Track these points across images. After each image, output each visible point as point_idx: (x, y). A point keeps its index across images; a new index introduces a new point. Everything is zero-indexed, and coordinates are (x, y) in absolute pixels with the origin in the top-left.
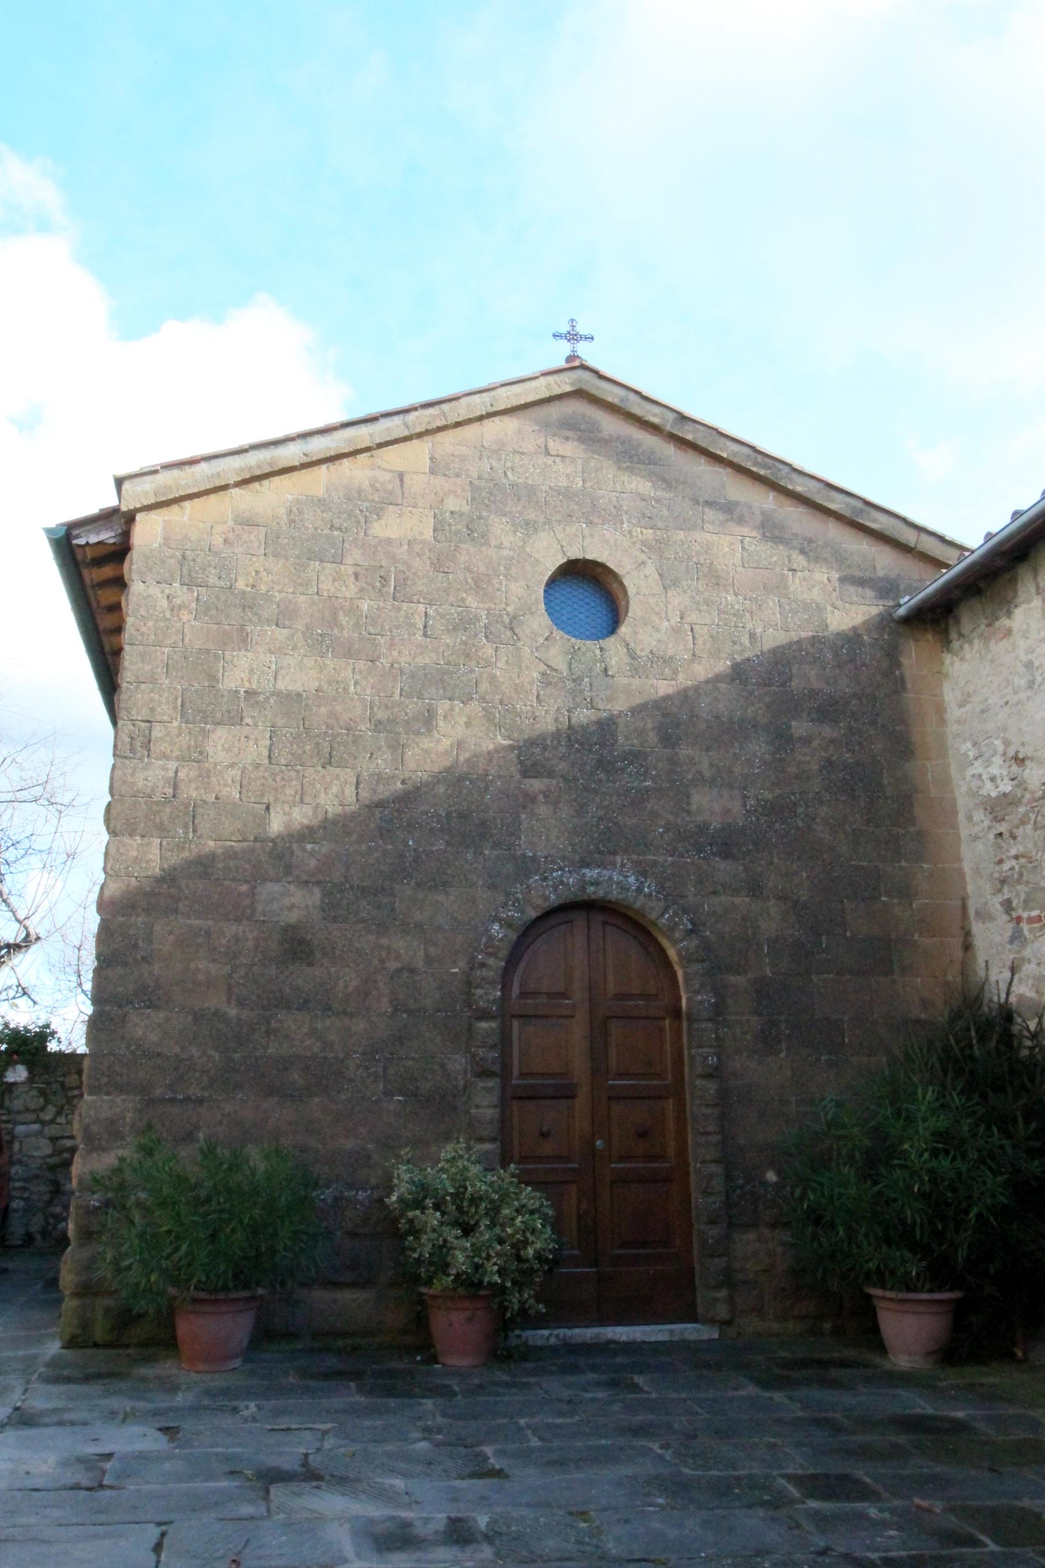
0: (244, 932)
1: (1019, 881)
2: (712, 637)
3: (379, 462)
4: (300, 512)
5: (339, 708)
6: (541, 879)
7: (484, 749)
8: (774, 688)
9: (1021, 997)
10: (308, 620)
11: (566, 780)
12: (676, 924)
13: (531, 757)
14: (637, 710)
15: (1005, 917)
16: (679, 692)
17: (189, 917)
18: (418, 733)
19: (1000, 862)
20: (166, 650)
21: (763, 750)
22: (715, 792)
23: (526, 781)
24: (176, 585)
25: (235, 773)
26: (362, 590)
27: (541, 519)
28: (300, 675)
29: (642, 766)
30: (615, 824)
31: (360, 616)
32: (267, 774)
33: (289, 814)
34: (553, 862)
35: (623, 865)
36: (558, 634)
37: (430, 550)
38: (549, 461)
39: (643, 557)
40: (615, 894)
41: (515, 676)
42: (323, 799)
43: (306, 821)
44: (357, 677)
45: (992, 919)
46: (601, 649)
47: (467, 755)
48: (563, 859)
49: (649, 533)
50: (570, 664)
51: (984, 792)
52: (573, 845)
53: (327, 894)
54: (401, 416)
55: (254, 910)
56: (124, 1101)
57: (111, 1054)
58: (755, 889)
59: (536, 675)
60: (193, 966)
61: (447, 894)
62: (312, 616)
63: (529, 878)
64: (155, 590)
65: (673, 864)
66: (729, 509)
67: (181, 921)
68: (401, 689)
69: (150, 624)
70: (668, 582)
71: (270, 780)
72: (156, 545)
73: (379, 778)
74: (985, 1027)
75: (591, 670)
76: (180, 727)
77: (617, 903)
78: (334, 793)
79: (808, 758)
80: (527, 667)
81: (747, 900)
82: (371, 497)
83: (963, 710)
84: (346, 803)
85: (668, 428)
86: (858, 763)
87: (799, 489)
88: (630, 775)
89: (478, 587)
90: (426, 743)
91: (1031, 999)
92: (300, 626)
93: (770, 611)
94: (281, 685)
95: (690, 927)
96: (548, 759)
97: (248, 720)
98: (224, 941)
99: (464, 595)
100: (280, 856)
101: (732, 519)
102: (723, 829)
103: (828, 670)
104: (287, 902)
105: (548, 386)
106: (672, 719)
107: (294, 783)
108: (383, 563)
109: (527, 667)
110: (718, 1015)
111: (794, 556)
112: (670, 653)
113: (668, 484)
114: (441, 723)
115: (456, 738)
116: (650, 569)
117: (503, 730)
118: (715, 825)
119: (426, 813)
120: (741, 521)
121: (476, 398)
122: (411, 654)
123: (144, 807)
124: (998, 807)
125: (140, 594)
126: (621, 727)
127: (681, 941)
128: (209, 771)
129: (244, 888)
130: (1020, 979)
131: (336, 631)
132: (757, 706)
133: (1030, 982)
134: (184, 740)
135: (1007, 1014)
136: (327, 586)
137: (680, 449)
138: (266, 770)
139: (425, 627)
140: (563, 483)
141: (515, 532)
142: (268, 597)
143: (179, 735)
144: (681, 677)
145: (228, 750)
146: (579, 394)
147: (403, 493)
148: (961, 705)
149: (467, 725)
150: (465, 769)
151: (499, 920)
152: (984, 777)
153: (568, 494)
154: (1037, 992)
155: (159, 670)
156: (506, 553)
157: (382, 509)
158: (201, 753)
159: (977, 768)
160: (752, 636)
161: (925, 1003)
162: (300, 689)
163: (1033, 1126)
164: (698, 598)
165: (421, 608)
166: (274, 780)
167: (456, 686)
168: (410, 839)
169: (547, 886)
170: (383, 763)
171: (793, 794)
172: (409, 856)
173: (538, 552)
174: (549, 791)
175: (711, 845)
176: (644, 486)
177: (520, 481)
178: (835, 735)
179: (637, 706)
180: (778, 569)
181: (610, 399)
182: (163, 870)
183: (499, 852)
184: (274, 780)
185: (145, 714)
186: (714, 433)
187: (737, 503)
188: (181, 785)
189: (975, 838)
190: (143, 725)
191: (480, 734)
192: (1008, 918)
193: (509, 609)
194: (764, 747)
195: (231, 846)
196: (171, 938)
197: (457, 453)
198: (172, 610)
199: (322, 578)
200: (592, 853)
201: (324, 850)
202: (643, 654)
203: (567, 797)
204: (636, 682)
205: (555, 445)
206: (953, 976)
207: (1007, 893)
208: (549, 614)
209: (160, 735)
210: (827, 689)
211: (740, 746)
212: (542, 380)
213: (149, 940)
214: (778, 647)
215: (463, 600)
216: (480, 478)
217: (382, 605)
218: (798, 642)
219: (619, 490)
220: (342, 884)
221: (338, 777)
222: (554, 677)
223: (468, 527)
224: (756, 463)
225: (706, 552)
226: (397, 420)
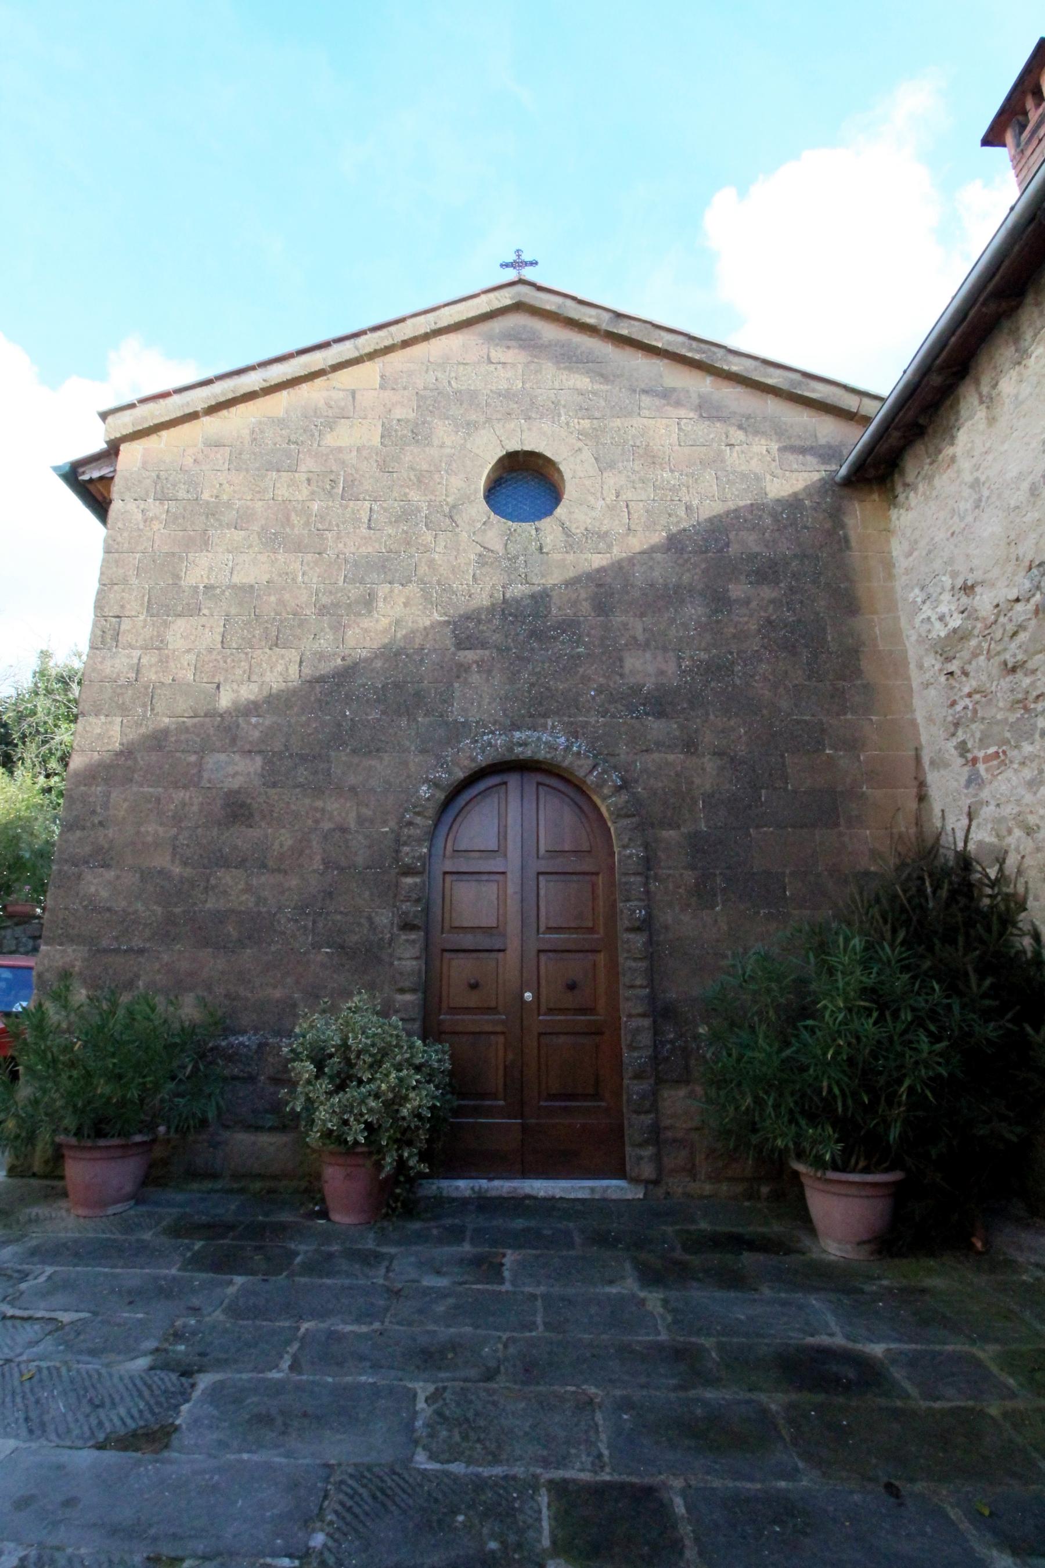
0: (191, 798)
1: (973, 720)
2: (647, 511)
3: (334, 383)
4: (262, 432)
5: (287, 596)
6: (471, 743)
7: (421, 626)
8: (712, 557)
9: (980, 843)
10: (263, 522)
11: (499, 649)
12: (605, 781)
13: (466, 631)
14: (568, 583)
15: (961, 761)
16: (613, 564)
17: (142, 786)
18: (360, 615)
19: (953, 703)
20: (138, 556)
21: (700, 613)
22: (648, 655)
23: (461, 653)
24: (150, 500)
25: (191, 657)
26: (313, 493)
27: (482, 419)
28: (254, 568)
29: (574, 634)
30: (547, 689)
31: (311, 515)
32: (219, 657)
33: (237, 692)
34: (485, 727)
35: (553, 727)
36: (495, 518)
37: (377, 454)
38: (492, 368)
39: (580, 444)
40: (543, 754)
41: (452, 558)
42: (269, 677)
43: (252, 697)
44: (305, 568)
45: (946, 765)
46: (537, 529)
47: (404, 632)
48: (495, 723)
49: (586, 423)
50: (506, 545)
51: (933, 635)
52: (504, 711)
53: (268, 762)
54: (352, 341)
55: (200, 777)
56: (74, 951)
57: (66, 909)
58: (690, 746)
59: (473, 557)
60: (143, 829)
61: (381, 759)
62: (267, 519)
63: (459, 742)
64: (131, 506)
65: (604, 725)
66: (666, 394)
67: (135, 789)
68: (345, 576)
69: (125, 534)
70: (604, 464)
71: (221, 662)
72: (135, 469)
73: (321, 656)
74: (939, 876)
75: (526, 549)
76: (145, 621)
77: (551, 764)
78: (279, 671)
79: (746, 619)
80: (464, 550)
81: (682, 756)
82: (326, 414)
83: (911, 559)
84: (289, 679)
85: (604, 326)
86: (799, 621)
87: (734, 368)
88: (563, 643)
89: (420, 482)
90: (366, 623)
91: (991, 844)
92: (256, 528)
93: (706, 484)
94: (236, 579)
95: (619, 783)
96: (483, 632)
97: (205, 611)
98: (172, 807)
99: (407, 490)
100: (226, 729)
101: (668, 404)
102: (657, 690)
103: (767, 534)
104: (230, 770)
105: (489, 303)
106: (605, 590)
107: (243, 664)
108: (334, 468)
109: (465, 551)
110: (649, 869)
111: (731, 432)
112: (604, 528)
113: (605, 378)
114: (381, 604)
115: (395, 617)
116: (587, 454)
117: (439, 608)
118: (649, 685)
119: (364, 686)
120: (678, 404)
121: (422, 318)
122: (356, 544)
123: (110, 690)
124: (947, 648)
125: (119, 510)
126: (555, 599)
127: (610, 797)
128: (168, 656)
129: (193, 758)
130: (979, 825)
131: (288, 530)
132: (693, 572)
133: (990, 826)
134: (149, 632)
135: (965, 862)
136: (283, 492)
137: (618, 347)
138: (219, 653)
139: (369, 520)
140: (503, 385)
141: (457, 432)
142: (229, 505)
143: (144, 627)
144: (615, 550)
145: (186, 638)
146: (518, 307)
147: (354, 407)
148: (909, 554)
149: (406, 605)
150: (402, 644)
151: (427, 781)
152: (933, 619)
153: (507, 395)
154: (998, 836)
155: (131, 573)
156: (448, 451)
157: (335, 422)
158: (162, 641)
159: (927, 611)
160: (688, 508)
161: (875, 854)
162: (253, 582)
163: (987, 982)
164: (633, 477)
165: (367, 504)
166: (225, 662)
167: (396, 570)
168: (346, 711)
169: (475, 748)
170: (325, 643)
171: (731, 653)
172: (346, 725)
173: (478, 448)
174: (483, 661)
175: (644, 705)
176: (582, 381)
177: (463, 388)
178: (774, 595)
179: (572, 579)
180: (715, 445)
181: (548, 307)
182: (122, 744)
183: (432, 719)
184: (225, 662)
185: (116, 610)
186: (649, 326)
187: (674, 390)
188: (143, 671)
189: (927, 685)
190: (114, 620)
191: (417, 613)
192: (963, 761)
193: (449, 500)
194: (700, 610)
195: (184, 722)
196: (126, 805)
197: (405, 369)
198: (145, 521)
199: (278, 485)
200: (523, 716)
201: (267, 722)
202: (577, 530)
203: (499, 666)
204: (570, 558)
205: (498, 354)
206: (904, 826)
207: (961, 735)
208: (487, 503)
209: (128, 628)
210: (766, 553)
211: (676, 611)
212: (483, 297)
213: (106, 806)
214: (715, 517)
215: (406, 494)
216: (425, 389)
217: (330, 504)
218: (736, 510)
219: (557, 387)
220: (281, 752)
221: (283, 657)
222: (490, 557)
223: (412, 432)
224: (691, 350)
225: (642, 436)
226: (348, 344)
